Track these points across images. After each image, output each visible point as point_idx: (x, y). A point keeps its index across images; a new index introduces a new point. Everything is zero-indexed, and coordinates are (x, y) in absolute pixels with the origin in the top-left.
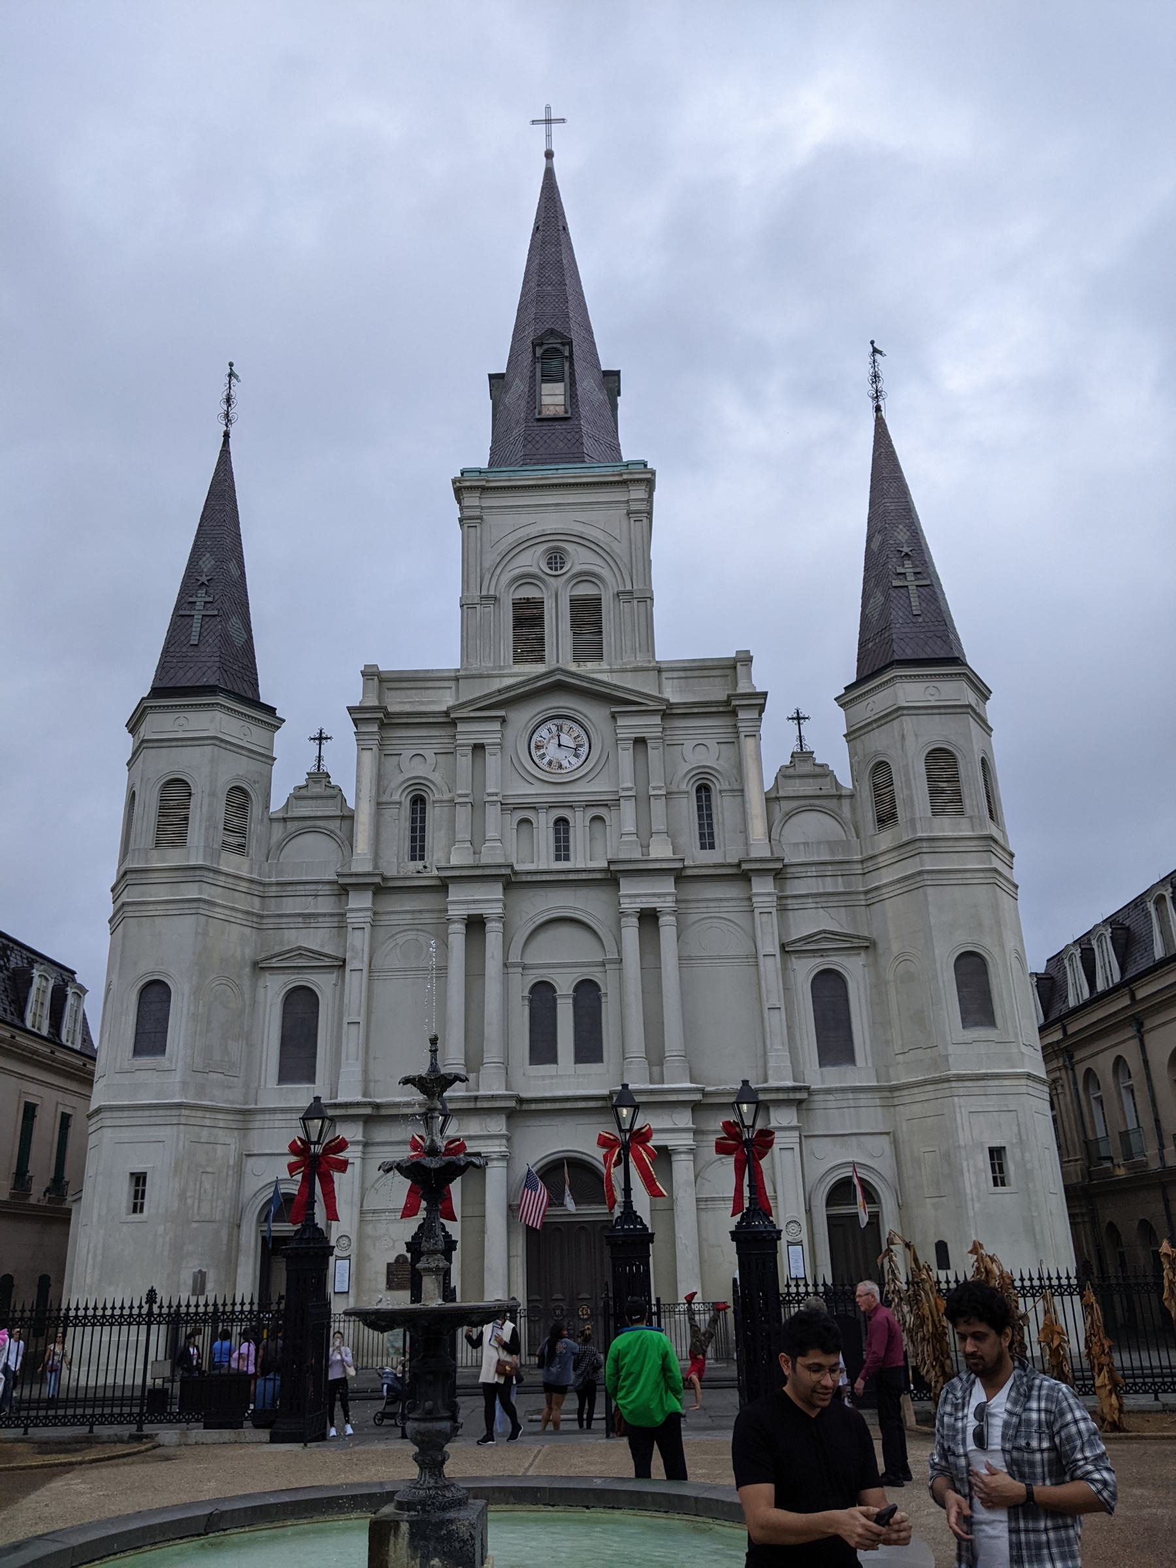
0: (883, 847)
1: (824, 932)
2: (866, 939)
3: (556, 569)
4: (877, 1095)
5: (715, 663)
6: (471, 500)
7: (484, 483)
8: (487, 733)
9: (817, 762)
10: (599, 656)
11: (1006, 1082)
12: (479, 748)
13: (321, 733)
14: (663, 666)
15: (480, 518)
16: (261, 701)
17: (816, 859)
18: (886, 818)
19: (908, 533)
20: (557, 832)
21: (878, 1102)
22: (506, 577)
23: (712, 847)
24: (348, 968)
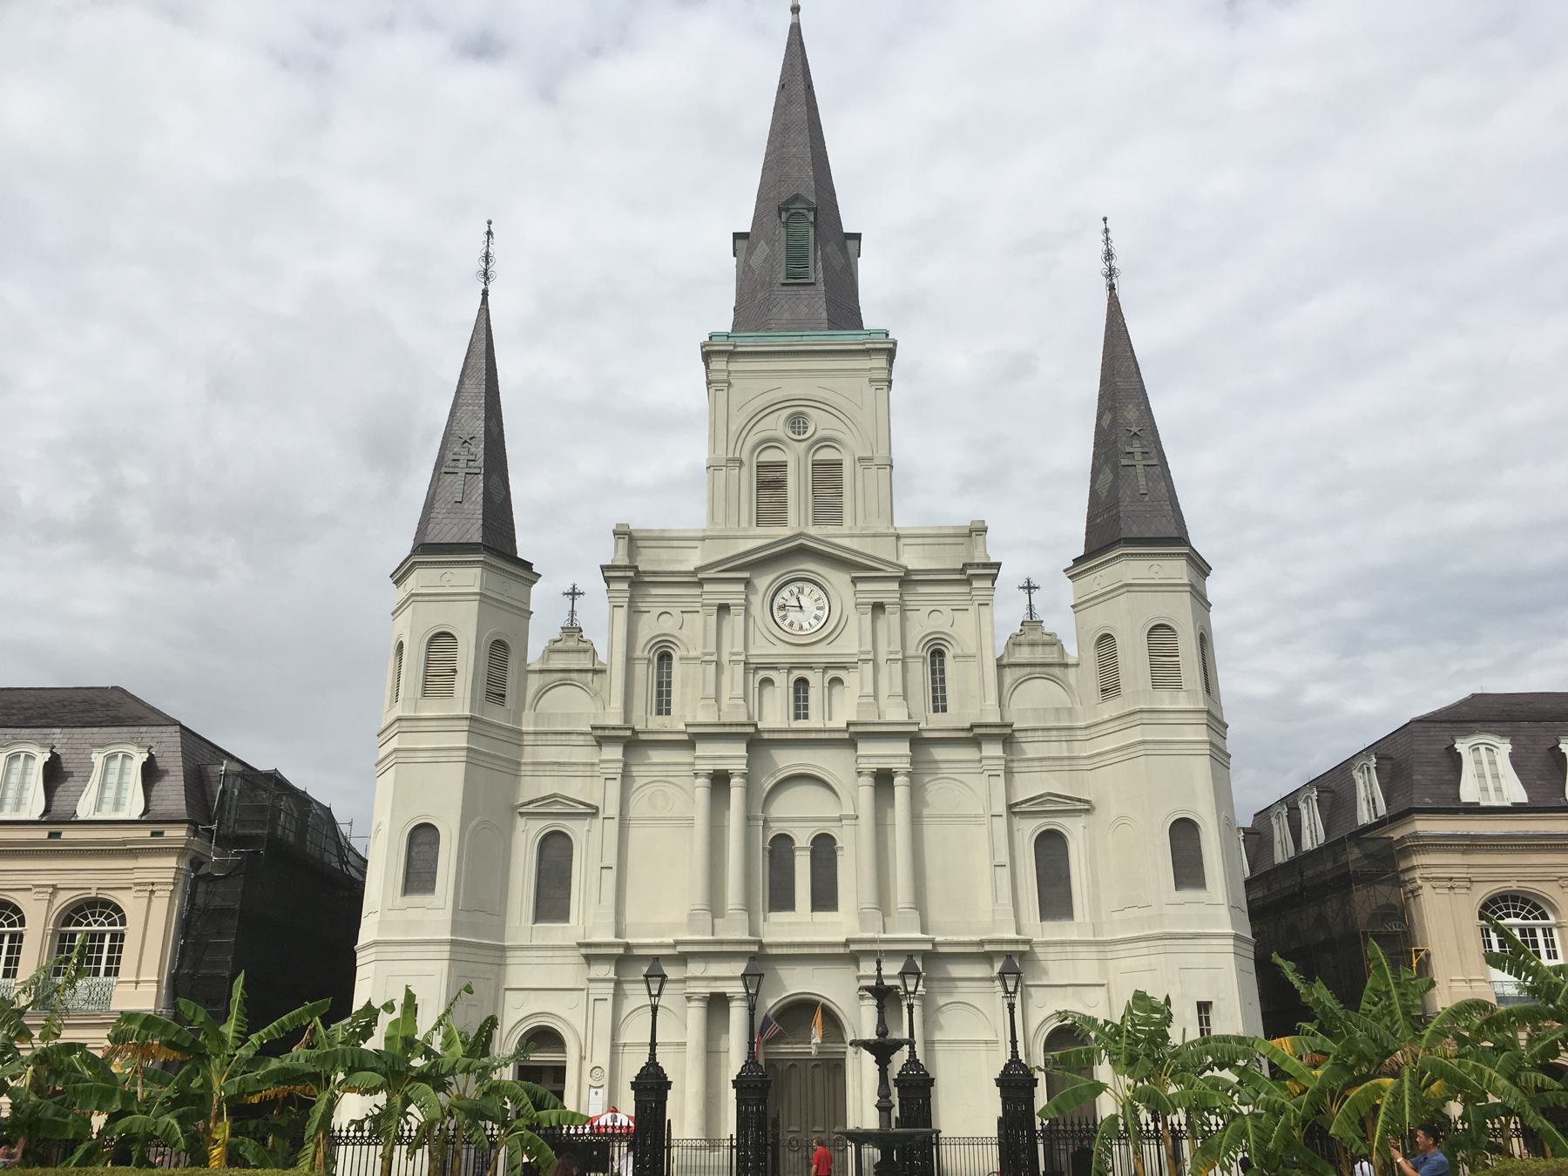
0: (1106, 717)
1: (1050, 794)
2: (1087, 802)
3: (799, 434)
4: (1094, 949)
5: (952, 531)
6: (718, 364)
7: (732, 348)
8: (732, 593)
9: (1047, 630)
10: (838, 520)
11: (1214, 942)
12: (723, 609)
13: (574, 589)
14: (900, 532)
15: (730, 384)
16: (518, 556)
17: (1042, 725)
18: (1109, 689)
19: (1137, 413)
20: (797, 691)
21: (1094, 956)
23: (944, 709)
24: (601, 815)
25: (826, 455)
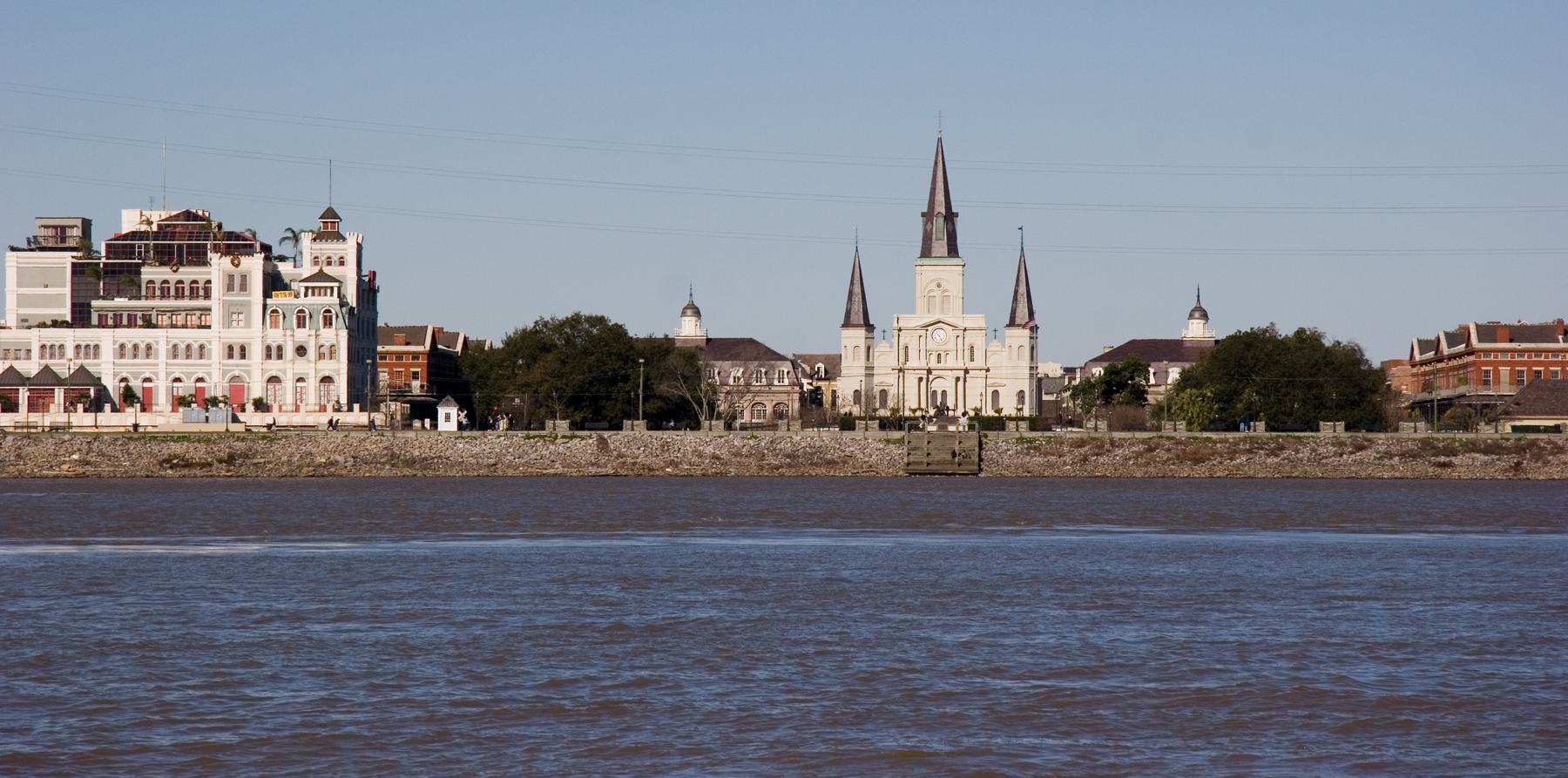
8: (923, 333)
16: (871, 323)
22: (928, 289)
25: (946, 294)
